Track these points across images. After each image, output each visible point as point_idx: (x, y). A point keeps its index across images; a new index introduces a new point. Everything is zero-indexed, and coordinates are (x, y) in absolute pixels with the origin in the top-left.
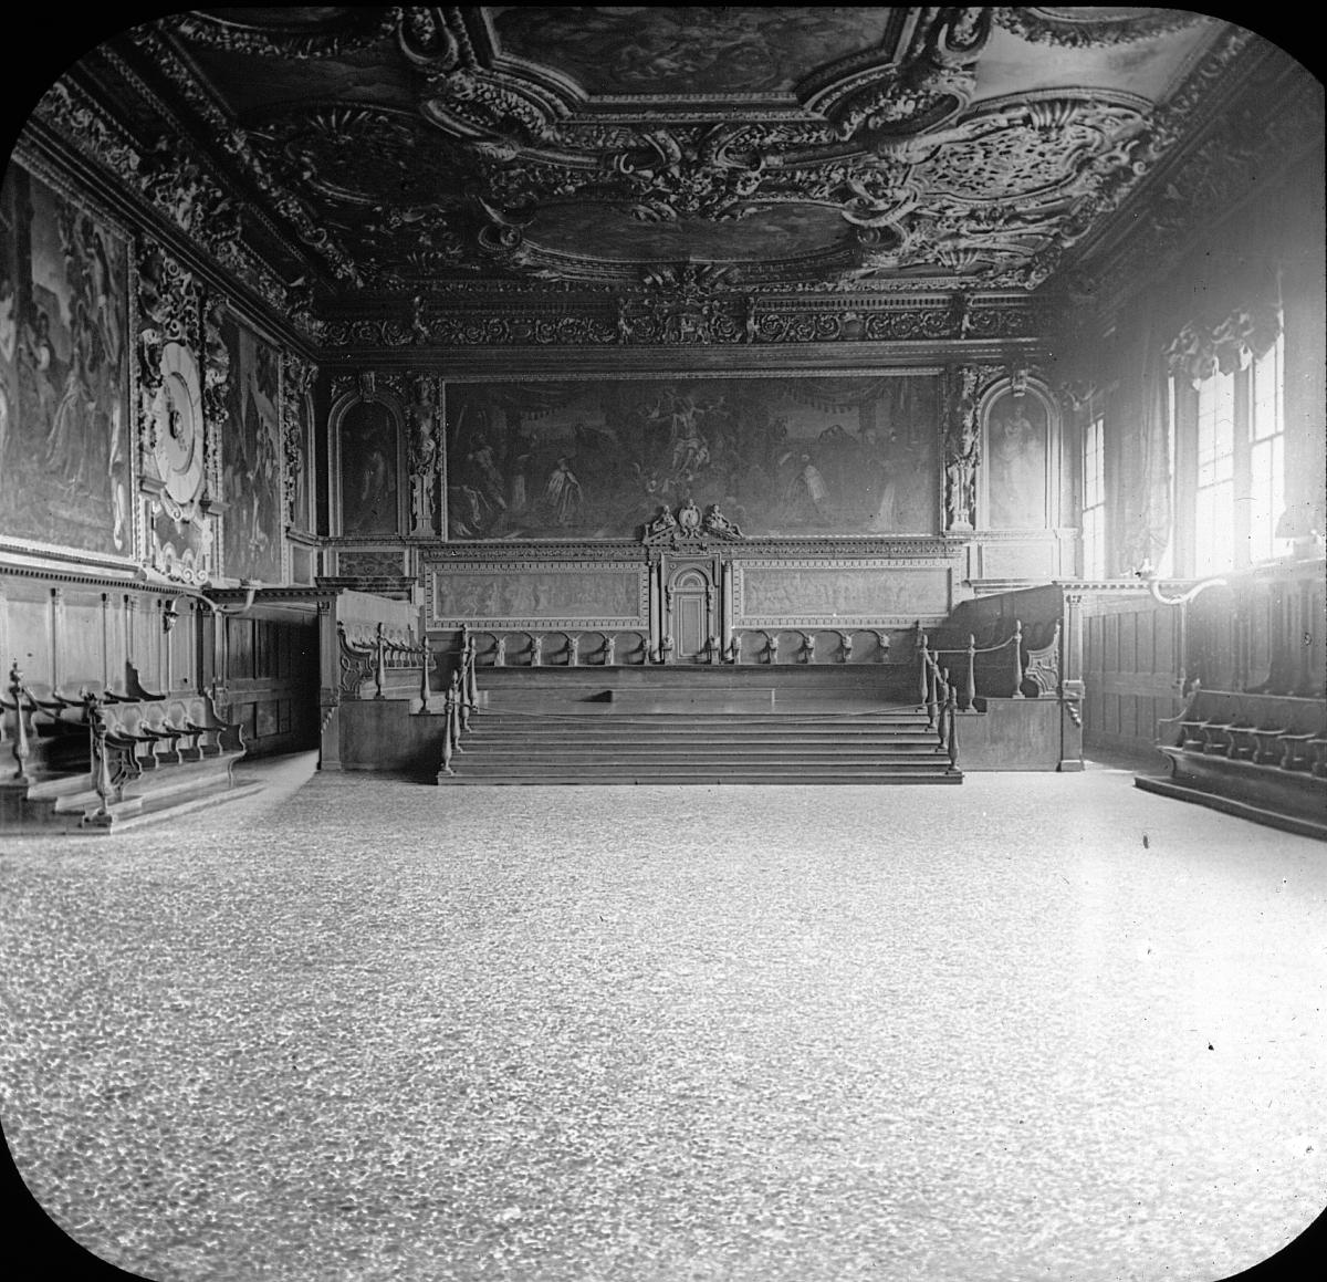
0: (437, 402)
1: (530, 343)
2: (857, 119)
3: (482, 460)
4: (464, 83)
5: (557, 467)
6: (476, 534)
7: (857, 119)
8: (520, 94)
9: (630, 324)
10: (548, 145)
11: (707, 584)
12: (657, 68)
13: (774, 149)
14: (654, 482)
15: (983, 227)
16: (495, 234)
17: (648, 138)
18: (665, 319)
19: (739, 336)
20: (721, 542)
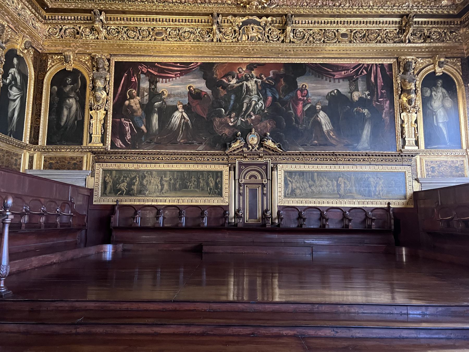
0: (109, 71)
1: (163, 40)
3: (133, 104)
5: (177, 109)
11: (262, 178)
14: (232, 120)
18: (240, 29)
20: (271, 152)
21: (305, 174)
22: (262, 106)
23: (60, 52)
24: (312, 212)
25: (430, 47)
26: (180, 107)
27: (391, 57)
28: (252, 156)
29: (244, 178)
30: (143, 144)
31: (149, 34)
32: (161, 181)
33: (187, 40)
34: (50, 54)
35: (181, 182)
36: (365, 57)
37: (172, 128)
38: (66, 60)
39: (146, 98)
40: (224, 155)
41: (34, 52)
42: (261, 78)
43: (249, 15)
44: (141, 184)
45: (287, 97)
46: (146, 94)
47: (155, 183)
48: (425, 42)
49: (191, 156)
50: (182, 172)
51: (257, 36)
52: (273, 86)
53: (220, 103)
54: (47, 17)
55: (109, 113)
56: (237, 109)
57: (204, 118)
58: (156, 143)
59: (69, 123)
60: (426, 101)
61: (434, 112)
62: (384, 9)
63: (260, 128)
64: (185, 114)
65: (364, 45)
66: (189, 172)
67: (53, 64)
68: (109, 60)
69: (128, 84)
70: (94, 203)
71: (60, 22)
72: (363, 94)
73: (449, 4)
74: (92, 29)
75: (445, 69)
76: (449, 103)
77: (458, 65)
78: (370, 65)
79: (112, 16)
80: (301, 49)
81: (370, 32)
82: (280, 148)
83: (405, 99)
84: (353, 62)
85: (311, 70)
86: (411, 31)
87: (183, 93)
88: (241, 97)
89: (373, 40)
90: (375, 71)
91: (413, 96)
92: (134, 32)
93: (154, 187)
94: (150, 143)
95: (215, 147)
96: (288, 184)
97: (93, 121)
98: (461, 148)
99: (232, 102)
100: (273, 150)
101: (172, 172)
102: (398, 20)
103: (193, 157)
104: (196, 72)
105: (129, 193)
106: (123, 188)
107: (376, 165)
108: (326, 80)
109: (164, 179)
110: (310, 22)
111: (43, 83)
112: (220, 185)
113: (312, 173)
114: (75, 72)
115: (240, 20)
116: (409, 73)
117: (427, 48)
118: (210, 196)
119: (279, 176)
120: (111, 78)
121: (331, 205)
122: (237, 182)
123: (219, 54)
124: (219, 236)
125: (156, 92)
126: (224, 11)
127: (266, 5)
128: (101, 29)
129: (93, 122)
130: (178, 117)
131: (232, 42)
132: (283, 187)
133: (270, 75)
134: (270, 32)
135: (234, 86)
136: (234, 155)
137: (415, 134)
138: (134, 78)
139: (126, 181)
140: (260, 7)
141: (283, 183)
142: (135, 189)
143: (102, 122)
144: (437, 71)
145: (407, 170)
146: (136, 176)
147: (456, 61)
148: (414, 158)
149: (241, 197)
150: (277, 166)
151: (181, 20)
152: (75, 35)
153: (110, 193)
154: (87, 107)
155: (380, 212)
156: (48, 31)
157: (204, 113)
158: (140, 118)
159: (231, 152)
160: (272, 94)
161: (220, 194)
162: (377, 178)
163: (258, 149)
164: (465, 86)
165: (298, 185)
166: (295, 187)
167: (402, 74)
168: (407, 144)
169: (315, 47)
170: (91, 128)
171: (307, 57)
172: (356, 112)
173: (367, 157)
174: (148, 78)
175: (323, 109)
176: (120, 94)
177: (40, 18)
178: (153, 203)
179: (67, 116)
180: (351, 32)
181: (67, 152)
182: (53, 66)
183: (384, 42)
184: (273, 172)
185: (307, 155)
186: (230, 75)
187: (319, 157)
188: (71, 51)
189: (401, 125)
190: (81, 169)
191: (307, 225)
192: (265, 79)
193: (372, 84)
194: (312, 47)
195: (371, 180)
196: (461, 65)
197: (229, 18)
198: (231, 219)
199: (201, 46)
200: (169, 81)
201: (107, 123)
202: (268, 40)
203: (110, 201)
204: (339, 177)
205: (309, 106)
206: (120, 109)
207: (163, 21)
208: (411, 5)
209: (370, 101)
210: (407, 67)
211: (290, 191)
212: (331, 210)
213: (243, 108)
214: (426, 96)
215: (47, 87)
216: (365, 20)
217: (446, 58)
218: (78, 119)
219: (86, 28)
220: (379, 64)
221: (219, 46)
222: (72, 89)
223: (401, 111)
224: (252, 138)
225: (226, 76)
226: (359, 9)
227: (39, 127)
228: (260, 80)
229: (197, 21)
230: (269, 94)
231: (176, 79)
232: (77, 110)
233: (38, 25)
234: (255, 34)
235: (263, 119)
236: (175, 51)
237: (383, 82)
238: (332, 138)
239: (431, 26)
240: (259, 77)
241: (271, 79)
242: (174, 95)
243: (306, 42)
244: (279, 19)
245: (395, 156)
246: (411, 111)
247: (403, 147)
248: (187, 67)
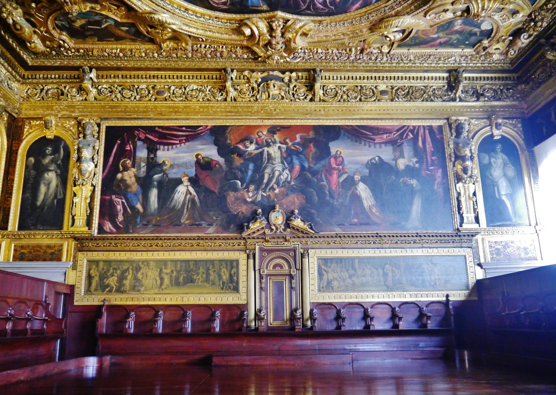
0: (98, 138)
1: (166, 100)
6: (119, 230)
9: (236, 89)
11: (290, 267)
14: (251, 194)
18: (259, 86)
19: (310, 96)
20: (301, 235)
21: (343, 261)
22: (287, 178)
23: (40, 116)
24: (353, 310)
25: (485, 106)
26: (185, 180)
27: (441, 117)
28: (276, 240)
29: (267, 268)
30: (138, 226)
31: (149, 93)
32: (160, 274)
33: (195, 100)
34: (27, 119)
35: (185, 275)
36: (410, 117)
37: (175, 206)
38: (46, 125)
39: (144, 170)
40: (240, 239)
41: (9, 117)
42: (286, 143)
43: (269, 70)
44: (136, 278)
45: (318, 165)
46: (143, 164)
47: (153, 276)
48: (478, 100)
49: (199, 241)
50: (187, 261)
51: (280, 94)
52: (301, 153)
53: (235, 174)
54: (26, 76)
55: (96, 189)
56: (257, 181)
57: (215, 193)
58: (153, 225)
59: (47, 203)
60: (485, 169)
61: (495, 182)
62: (428, 64)
63: (286, 204)
64: (191, 190)
66: (196, 262)
67: (30, 131)
68: (99, 125)
69: (122, 153)
70: (75, 304)
71: (41, 81)
72: (410, 161)
73: (501, 58)
74: (81, 89)
75: (503, 131)
76: (511, 172)
77: (519, 127)
78: (417, 128)
79: (105, 73)
80: (334, 108)
81: (414, 89)
82: (311, 228)
83: (459, 167)
84: (396, 123)
85: (346, 134)
86: (461, 88)
87: (190, 162)
88: (261, 166)
89: (418, 98)
90: (423, 134)
91: (468, 163)
92: (131, 91)
93: (151, 281)
94: (147, 225)
95: (229, 228)
96: (323, 275)
97: (76, 200)
98: (530, 225)
99: (250, 173)
100: (302, 232)
101: (175, 261)
102: (446, 75)
103: (201, 242)
104: (206, 136)
105: (119, 290)
106: (112, 283)
107: (430, 248)
108: (365, 145)
109: (165, 271)
110: (343, 77)
111: (17, 154)
112: (235, 278)
113: (352, 259)
114: (57, 140)
115: (259, 76)
116: (462, 136)
117: (481, 107)
118: (223, 291)
119: (311, 264)
120: (101, 146)
121: (376, 300)
122: (257, 273)
123: (233, 116)
124: (235, 343)
125: (156, 162)
126: (238, 66)
127: (288, 60)
128: (91, 89)
129: (77, 200)
130: (181, 193)
131: (250, 101)
132: (316, 278)
133: (296, 139)
134: (295, 89)
135: (252, 153)
136: (253, 238)
137: (475, 210)
138: (128, 146)
139: (115, 274)
140: (282, 61)
141: (316, 273)
142: (128, 285)
143: (88, 201)
144: (495, 134)
145: (468, 252)
146: (128, 269)
147: (516, 121)
148: (474, 238)
149: (263, 293)
150: (308, 252)
151: (187, 77)
152: (58, 96)
153: (96, 290)
154: (70, 182)
155: (437, 307)
156: (27, 92)
157: (215, 186)
158: (136, 194)
159: (249, 235)
160: (300, 163)
161: (236, 289)
162: (432, 264)
163: (284, 230)
164: (528, 151)
165: (335, 275)
166: (332, 278)
167: (455, 137)
168: (465, 220)
169: (350, 107)
170: (74, 207)
171: (341, 118)
172: (403, 184)
173: (418, 239)
174: (145, 145)
175: (364, 180)
176: (111, 166)
177: (18, 77)
178: (150, 303)
179: (45, 193)
180: (392, 88)
181: (42, 238)
182: (30, 133)
183: (432, 101)
184: (304, 259)
185: (344, 237)
186: (248, 140)
187: (360, 239)
188: (53, 115)
189: (458, 198)
190: (59, 259)
191: (347, 326)
192: (290, 144)
193: (420, 149)
194: (346, 107)
195: (425, 266)
196: (522, 127)
197: (246, 73)
198: (251, 321)
199: (212, 107)
200: (172, 148)
201: (94, 202)
202: (293, 99)
203: (94, 300)
204: (386, 264)
205: (345, 176)
206: (111, 184)
207: (165, 78)
208: (458, 60)
209: (418, 170)
210: (459, 129)
211: (325, 284)
212: (376, 306)
213: (264, 179)
214: (484, 163)
215: (22, 159)
216: (408, 75)
217: (504, 118)
218: (59, 197)
219: (73, 87)
220: (427, 126)
221: (234, 106)
222: (52, 161)
223: (456, 182)
224: (276, 217)
225: (242, 141)
226: (399, 64)
227: (10, 208)
228: (284, 146)
229: (207, 77)
230: (296, 162)
231: (181, 146)
232: (57, 186)
233: (15, 85)
234: (278, 92)
235: (289, 193)
236: (180, 112)
237: (433, 147)
238: (376, 215)
239: (485, 82)
240: (283, 142)
241: (298, 144)
242: (179, 166)
243: (339, 101)
244: (305, 74)
245: (452, 236)
246: (467, 182)
247: (461, 226)
248: (195, 132)
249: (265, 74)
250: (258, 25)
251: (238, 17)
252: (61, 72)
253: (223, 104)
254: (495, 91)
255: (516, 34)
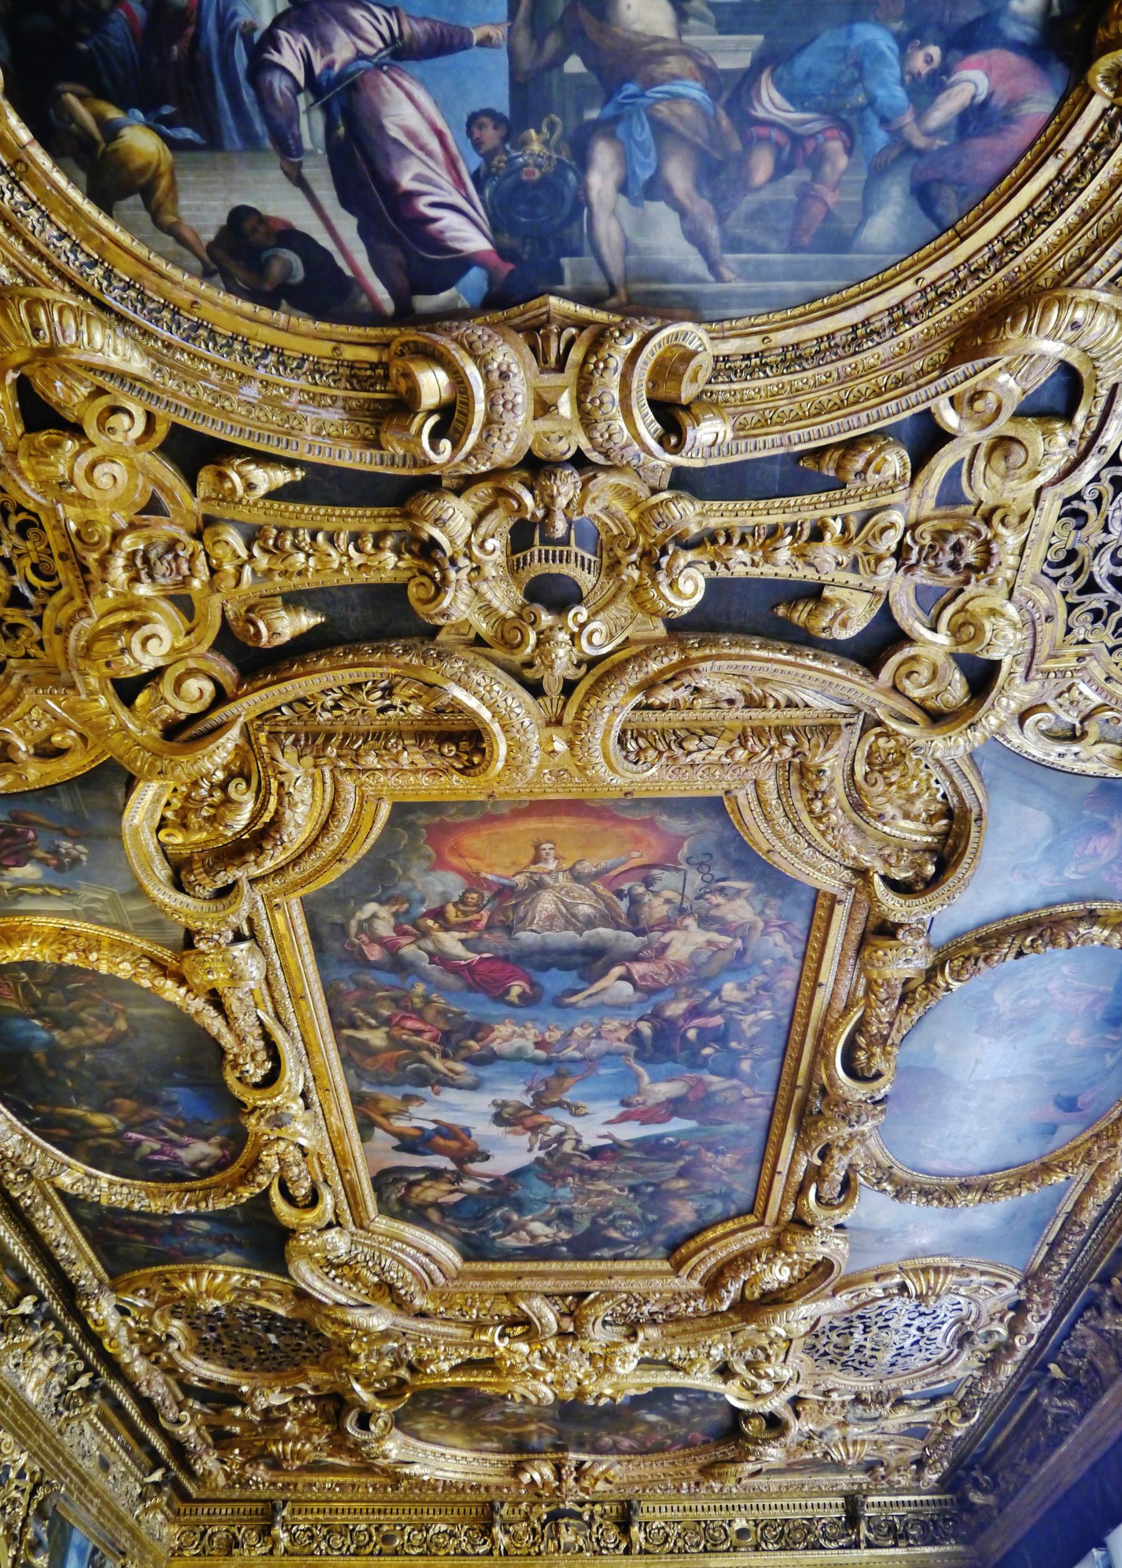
1: (396, 1553)
2: (733, 1289)
4: (339, 1242)
7: (733, 1289)
8: (394, 1257)
9: (507, 1532)
10: (422, 1315)
12: (529, 1233)
13: (654, 1322)
15: (873, 1413)
16: (364, 1422)
17: (524, 1306)
19: (623, 1545)
48: (895, 1546)
65: (783, 1556)
183: (822, 1548)
197: (524, 1506)
249: (553, 1508)
250: (541, 1472)
251: (514, 1457)
252: (236, 1506)
253: (487, 1561)
254: (924, 1524)
255: (921, 1463)
